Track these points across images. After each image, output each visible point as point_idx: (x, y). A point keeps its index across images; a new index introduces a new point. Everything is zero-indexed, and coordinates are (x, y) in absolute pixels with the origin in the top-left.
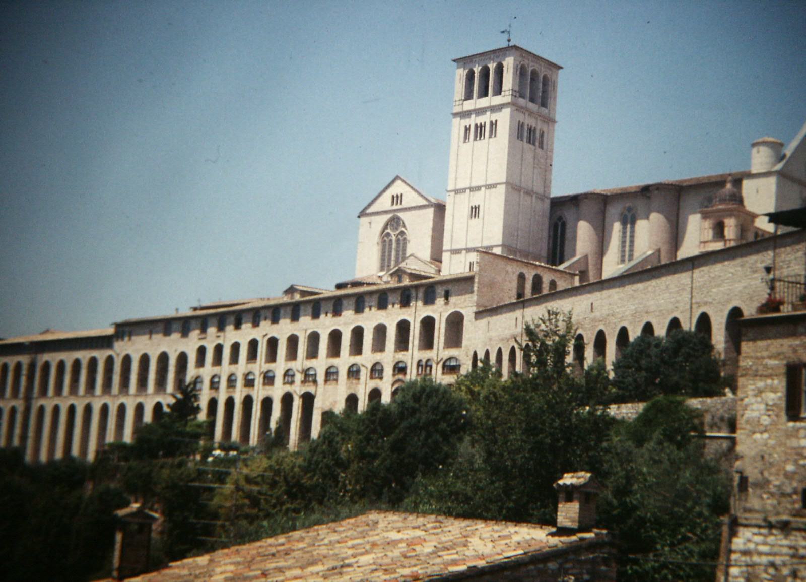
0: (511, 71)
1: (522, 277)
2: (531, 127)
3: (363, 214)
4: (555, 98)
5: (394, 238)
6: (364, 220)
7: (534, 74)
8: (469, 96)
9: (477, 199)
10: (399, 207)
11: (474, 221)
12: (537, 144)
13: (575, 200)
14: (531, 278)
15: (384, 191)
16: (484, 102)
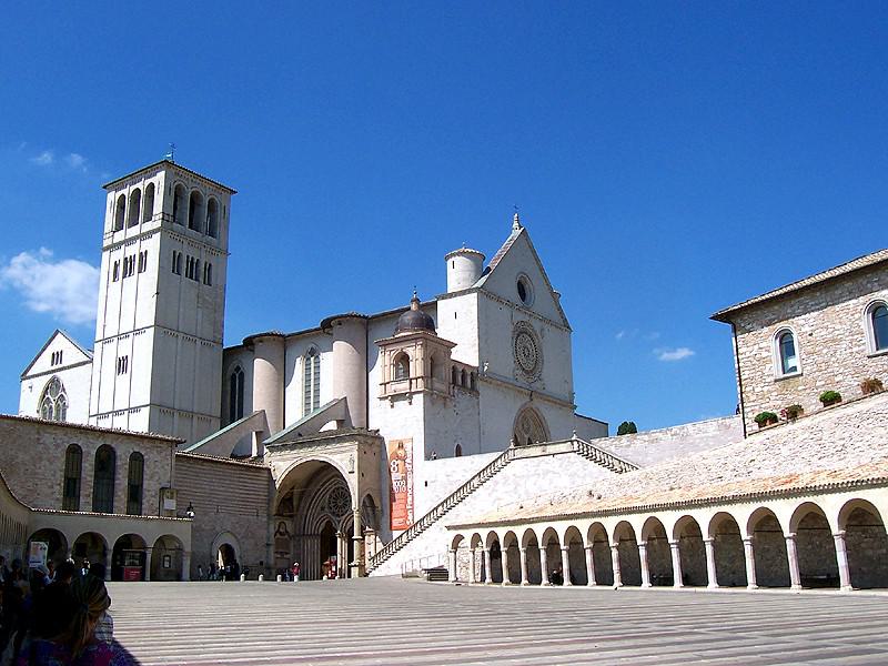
0: (162, 189)
1: (74, 452)
2: (193, 259)
3: (24, 377)
4: (227, 228)
5: (53, 405)
6: (26, 384)
7: (195, 200)
8: (119, 227)
9: (124, 348)
10: (59, 366)
11: (124, 377)
12: (201, 279)
13: (250, 343)
14: (94, 452)
15: (44, 350)
16: (134, 231)
